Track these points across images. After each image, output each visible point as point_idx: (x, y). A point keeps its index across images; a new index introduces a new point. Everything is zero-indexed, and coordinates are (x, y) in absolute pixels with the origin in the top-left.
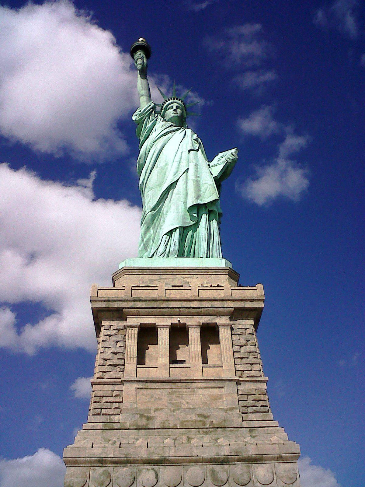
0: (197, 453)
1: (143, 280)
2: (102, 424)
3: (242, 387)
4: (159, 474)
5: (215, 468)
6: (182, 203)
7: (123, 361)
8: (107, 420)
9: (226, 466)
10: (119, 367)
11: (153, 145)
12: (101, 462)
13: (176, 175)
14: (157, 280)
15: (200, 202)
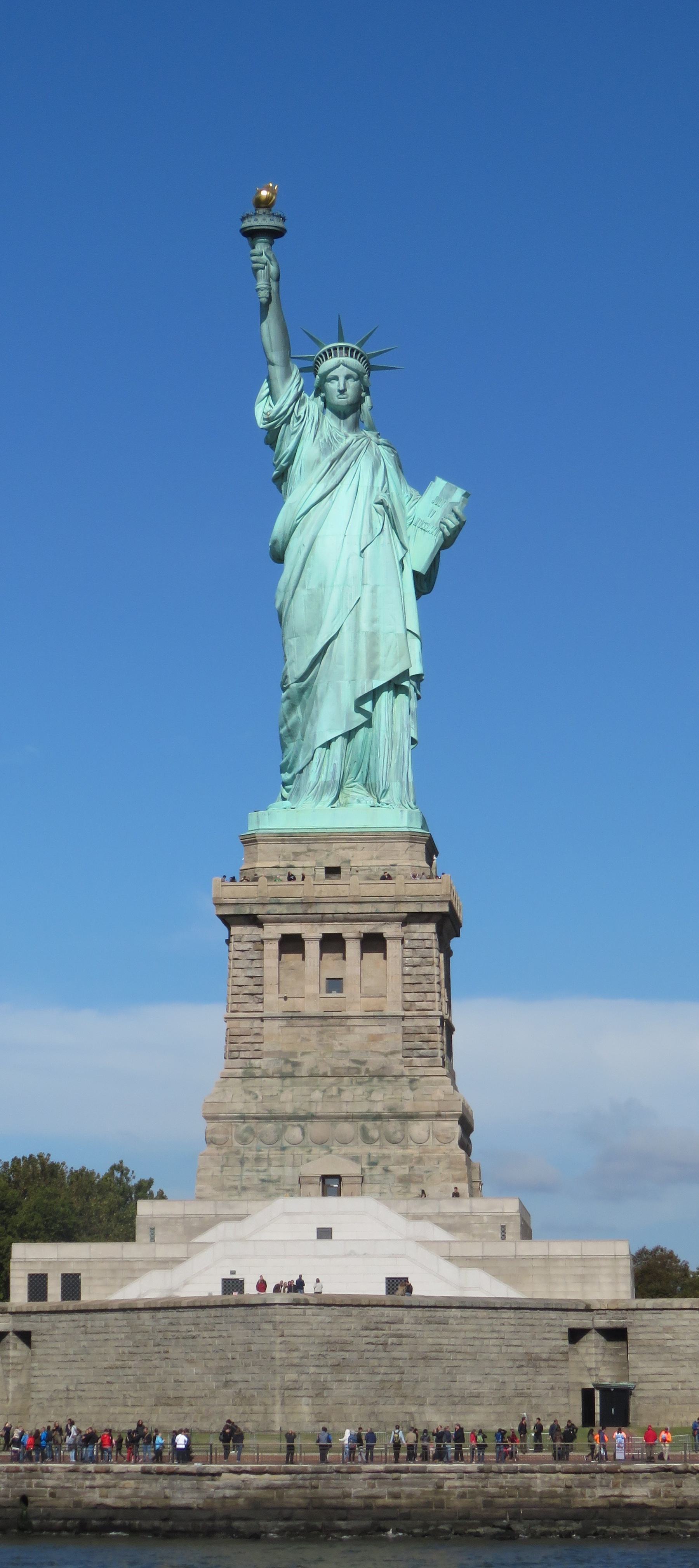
0: (346, 1109)
1: (284, 854)
2: (240, 1070)
3: (407, 1023)
4: (306, 1131)
5: (366, 1125)
6: (347, 682)
7: (261, 988)
8: (246, 1065)
9: (378, 1123)
10: (256, 997)
11: (297, 525)
12: (243, 1118)
13: (336, 620)
14: (304, 853)
15: (377, 683)
